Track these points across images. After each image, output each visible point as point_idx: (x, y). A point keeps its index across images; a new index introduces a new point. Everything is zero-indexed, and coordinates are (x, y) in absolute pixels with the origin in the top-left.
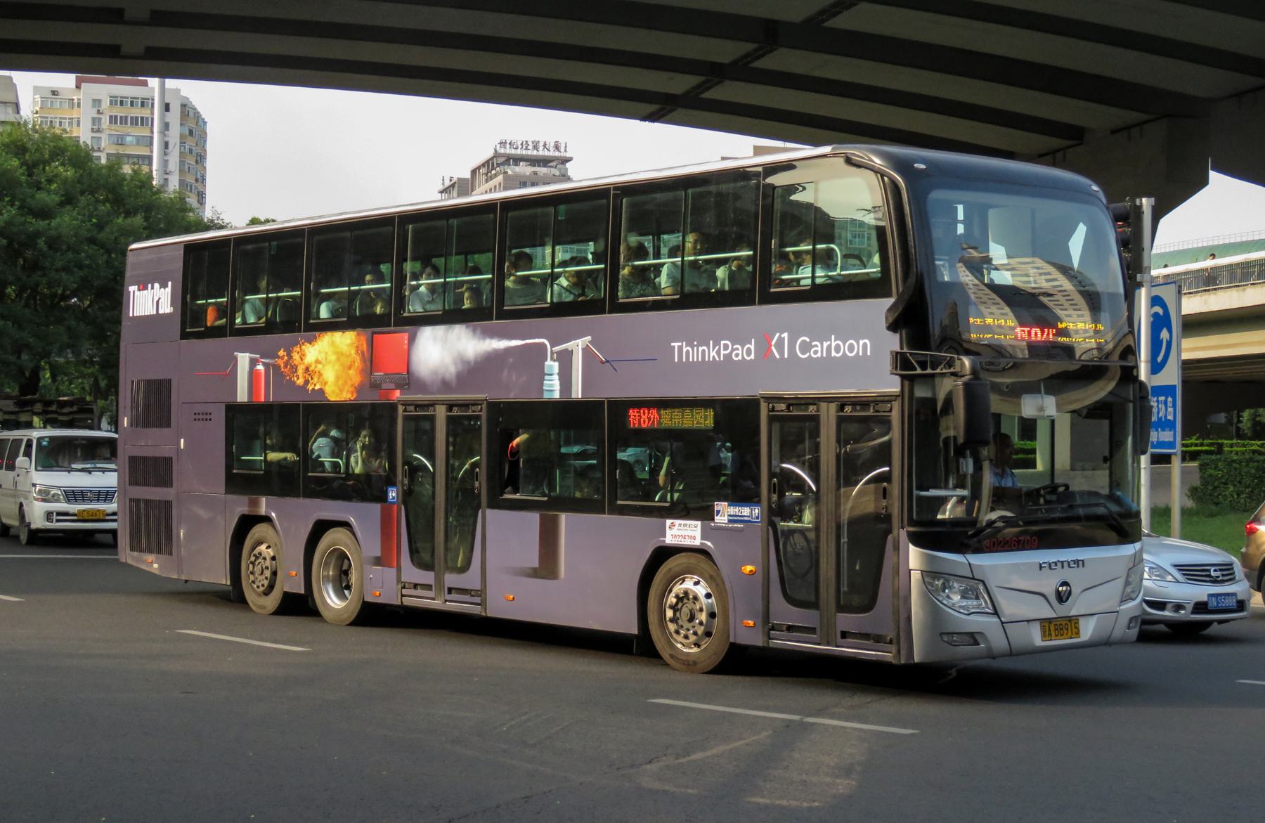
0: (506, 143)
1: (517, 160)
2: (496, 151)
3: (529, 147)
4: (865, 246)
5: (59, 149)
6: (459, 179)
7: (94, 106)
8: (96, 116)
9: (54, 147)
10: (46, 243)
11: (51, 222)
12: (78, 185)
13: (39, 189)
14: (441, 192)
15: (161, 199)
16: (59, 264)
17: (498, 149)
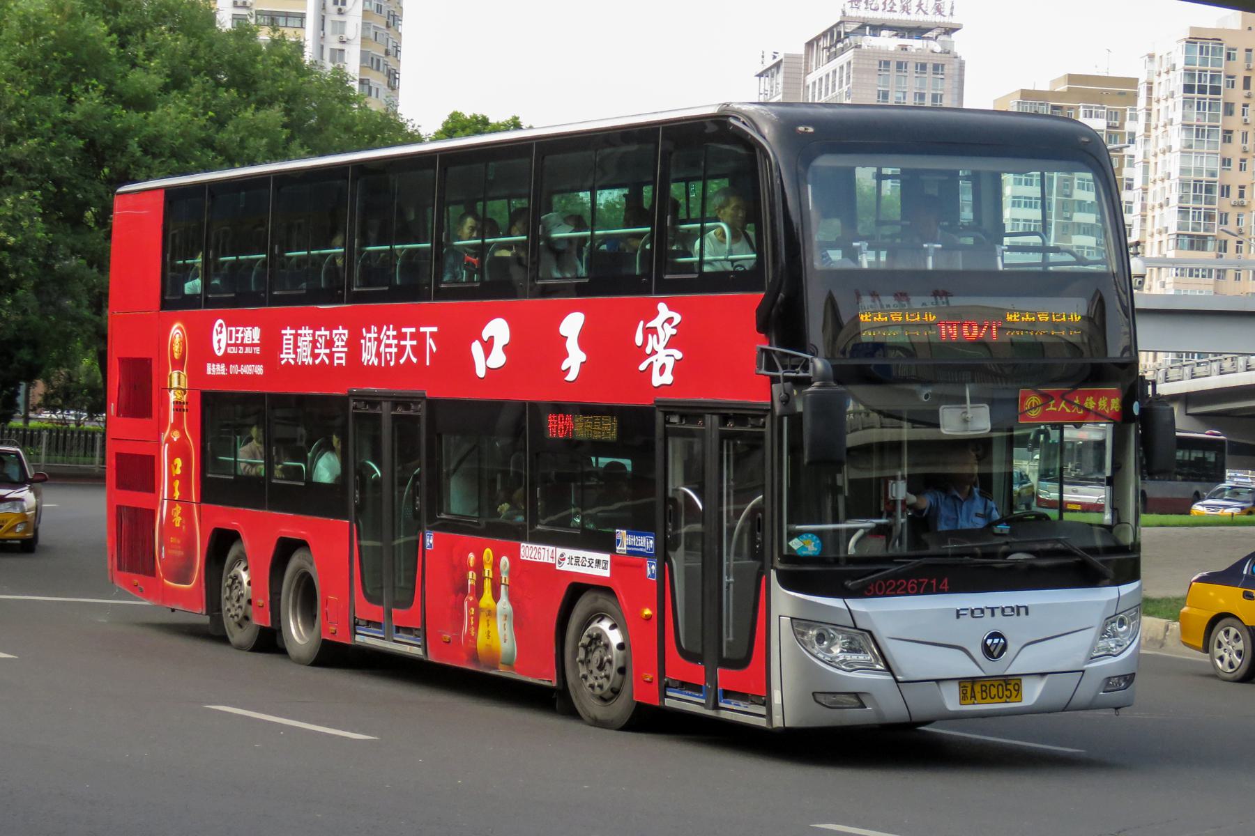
1: (876, 28)
2: (844, 12)
3: (895, 9)
5: (167, 7)
6: (787, 56)
10: (140, 145)
11: (147, 114)
12: (192, 61)
13: (134, 65)
14: (760, 75)
15: (310, 82)
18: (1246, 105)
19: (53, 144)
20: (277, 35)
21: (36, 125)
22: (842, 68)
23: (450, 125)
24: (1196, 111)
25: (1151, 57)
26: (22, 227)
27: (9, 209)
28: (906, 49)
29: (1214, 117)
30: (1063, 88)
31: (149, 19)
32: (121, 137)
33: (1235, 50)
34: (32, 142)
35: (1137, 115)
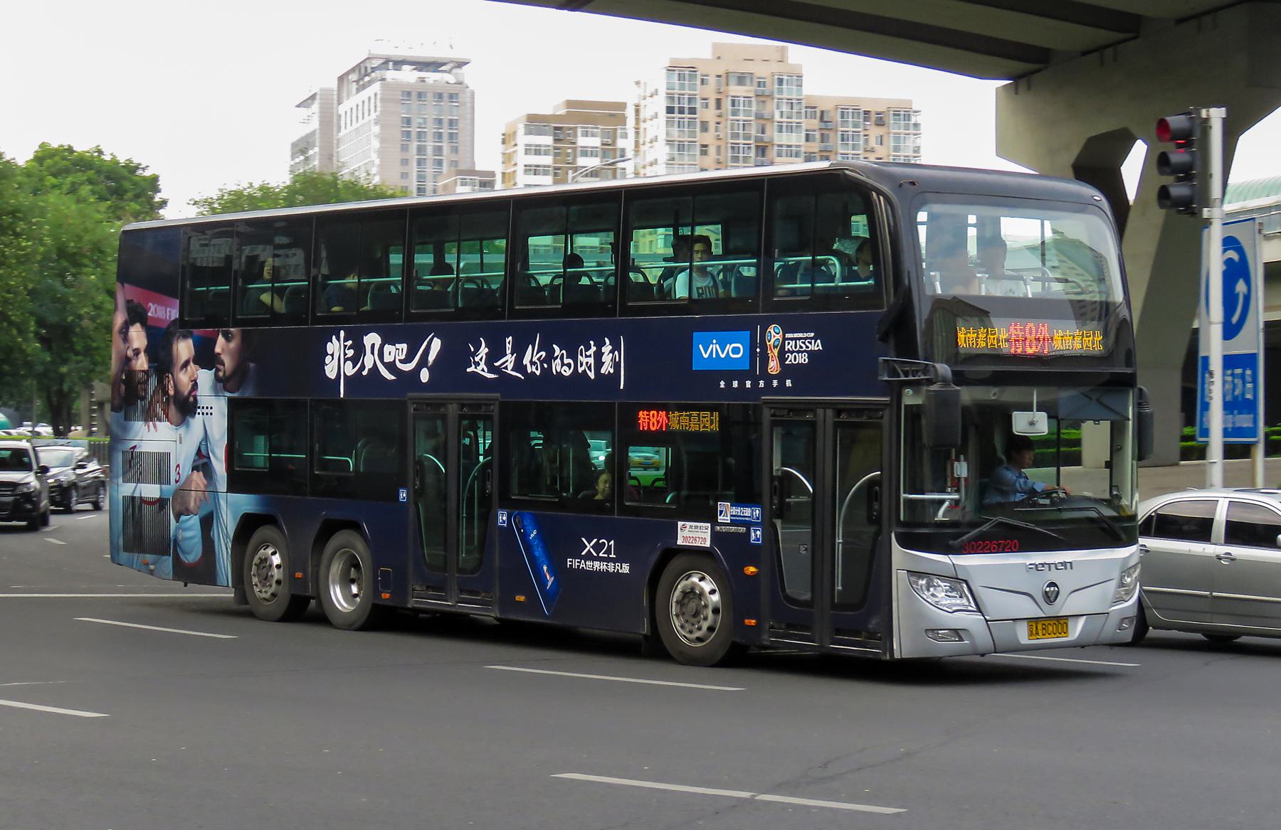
1: (398, 64)
22: (369, 98)
23: (40, 154)
25: (638, 83)
28: (424, 81)
29: (693, 134)
30: (562, 112)
33: (707, 76)
35: (626, 134)
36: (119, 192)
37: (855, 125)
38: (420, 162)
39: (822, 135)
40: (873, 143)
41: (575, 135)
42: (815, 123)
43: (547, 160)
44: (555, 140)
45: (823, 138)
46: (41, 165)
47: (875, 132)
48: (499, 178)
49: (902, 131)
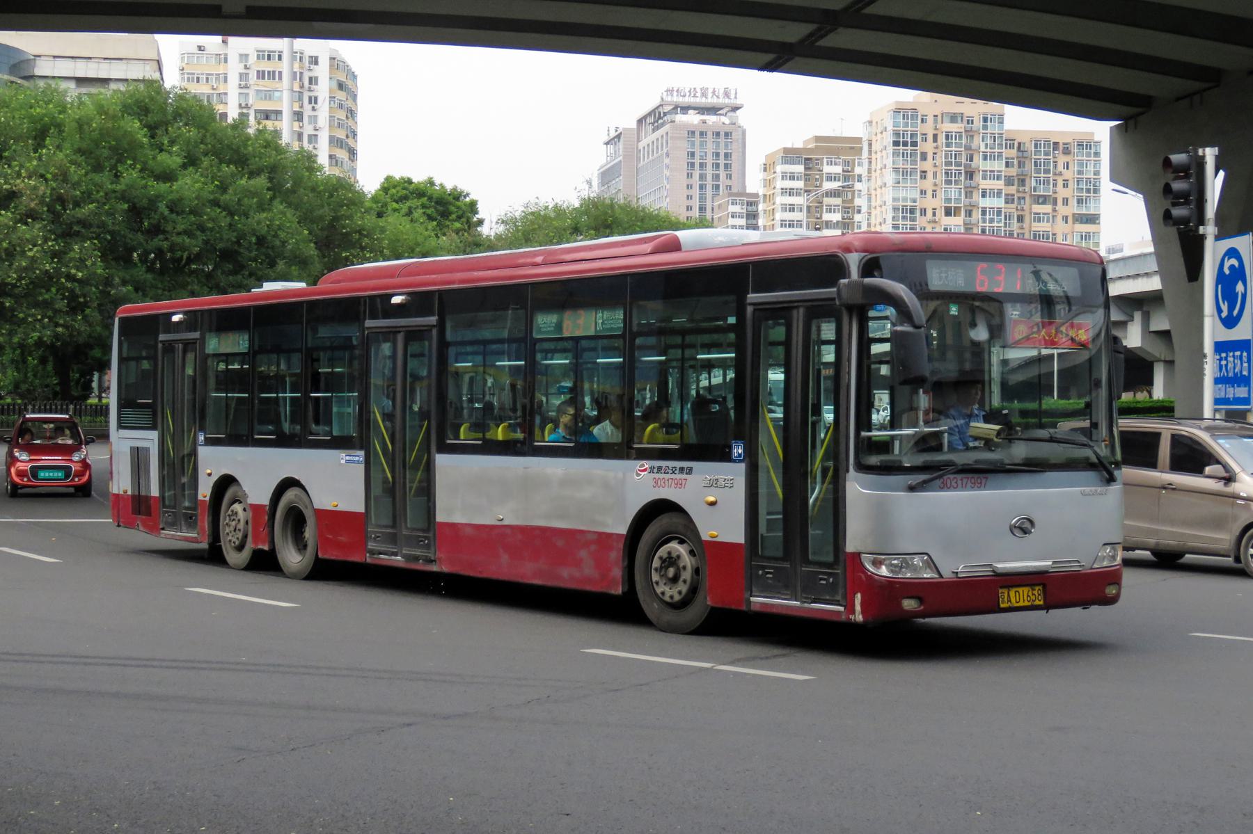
0: (673, 90)
2: (662, 99)
3: (697, 95)
4: (1051, 194)
5: (182, 109)
6: (624, 129)
7: (241, 61)
8: (244, 71)
9: (178, 107)
10: (167, 207)
11: (172, 185)
13: (161, 150)
14: (607, 143)
15: (286, 158)
16: (180, 228)
17: (664, 97)
18: (935, 154)
19: (106, 207)
20: (261, 127)
21: (92, 194)
23: (386, 185)
24: (901, 158)
25: (870, 122)
26: (86, 265)
27: (77, 253)
31: (170, 117)
32: (153, 201)
34: (90, 206)
36: (445, 214)
37: (1047, 154)
38: (701, 187)
39: (1019, 162)
40: (1060, 168)
41: (822, 165)
42: (1014, 152)
43: (800, 184)
44: (806, 169)
45: (1020, 165)
46: (387, 194)
47: (1062, 159)
48: (761, 199)
49: (1085, 158)
